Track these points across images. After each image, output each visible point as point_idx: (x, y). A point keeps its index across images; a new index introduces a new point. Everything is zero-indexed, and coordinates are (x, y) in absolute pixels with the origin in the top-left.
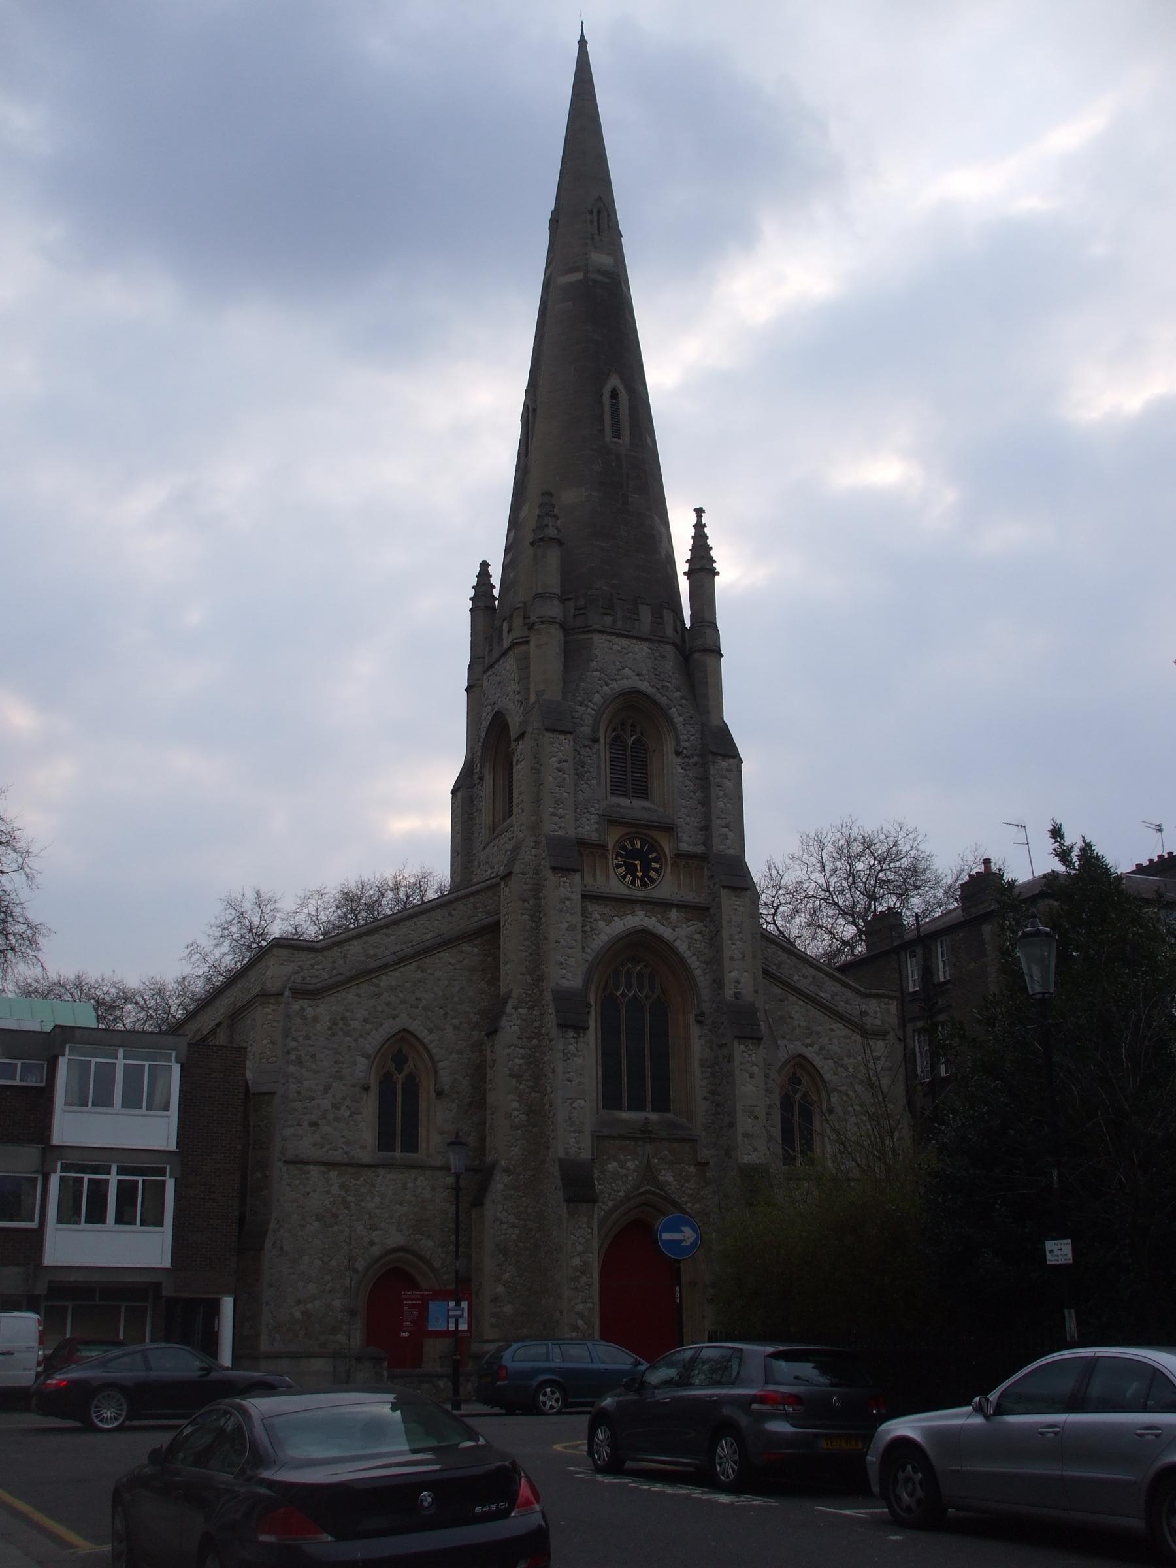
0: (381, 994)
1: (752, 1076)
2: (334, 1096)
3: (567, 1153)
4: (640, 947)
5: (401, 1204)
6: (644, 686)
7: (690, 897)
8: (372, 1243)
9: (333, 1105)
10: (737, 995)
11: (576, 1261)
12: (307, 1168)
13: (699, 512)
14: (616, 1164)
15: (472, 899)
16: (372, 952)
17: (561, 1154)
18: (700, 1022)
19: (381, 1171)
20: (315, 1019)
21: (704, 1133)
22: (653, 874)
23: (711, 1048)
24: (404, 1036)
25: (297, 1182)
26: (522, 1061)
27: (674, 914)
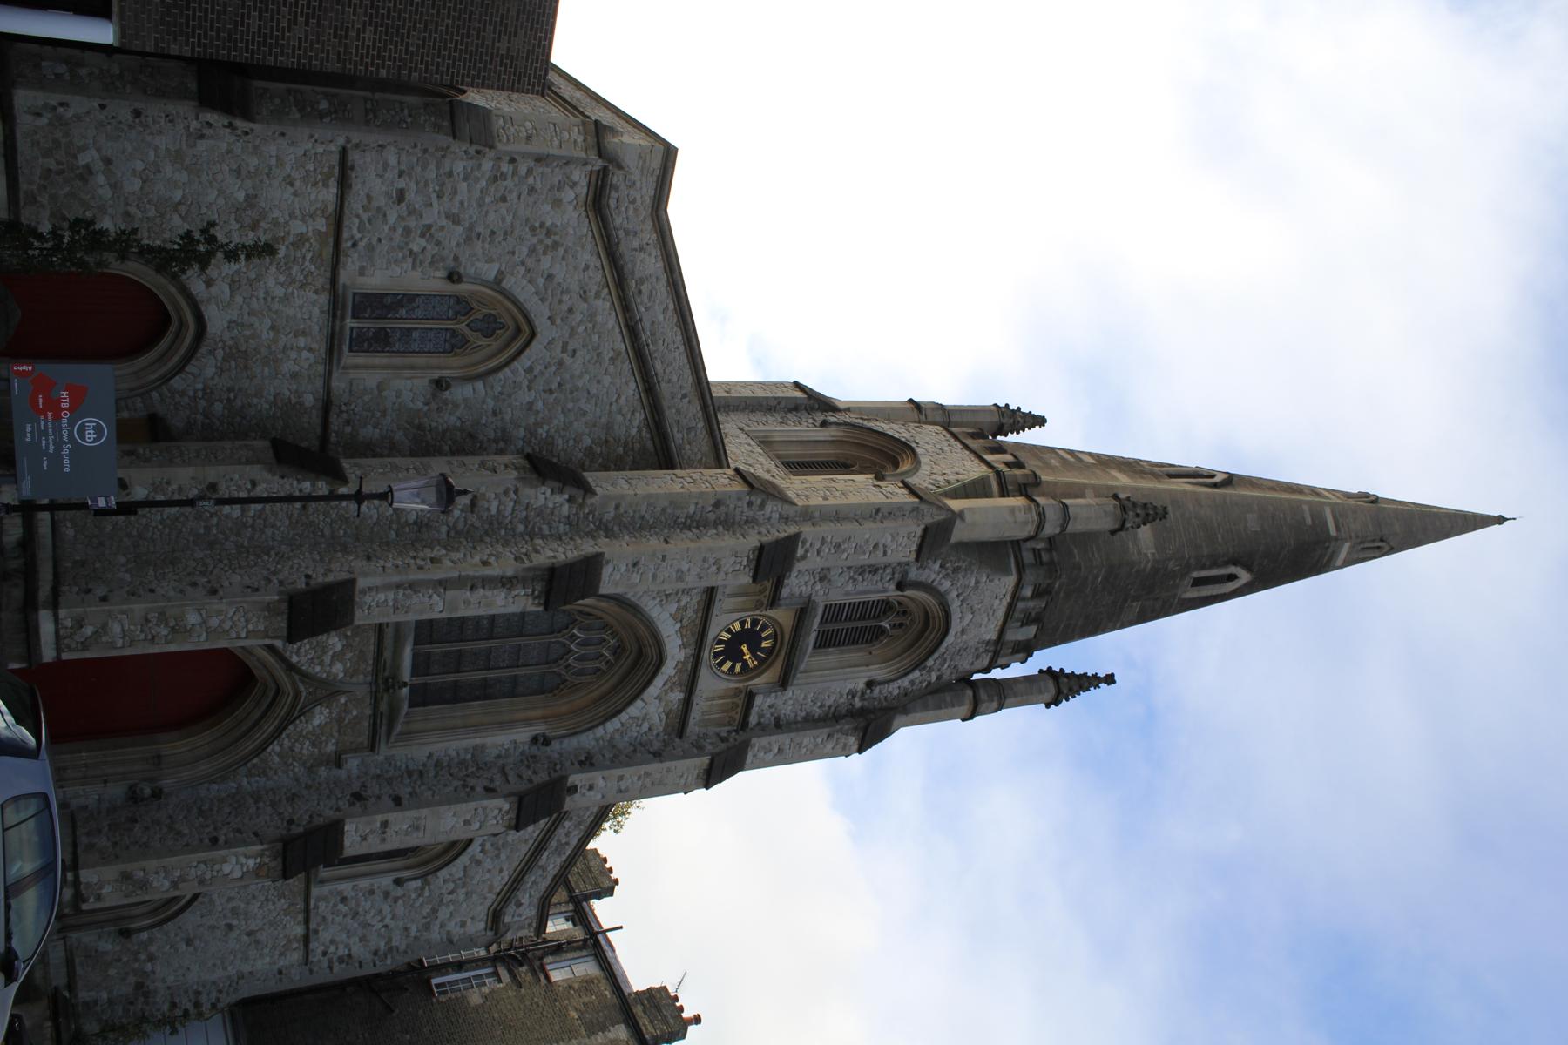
0: (585, 300)
1: (467, 823)
2: (442, 228)
3: (363, 592)
4: (641, 658)
5: (273, 328)
6: (950, 639)
7: (696, 714)
8: (209, 283)
9: (429, 227)
10: (573, 789)
11: (193, 618)
12: (333, 183)
13: (1110, 679)
14: (339, 647)
15: (701, 425)
16: (645, 288)
17: (362, 583)
18: (535, 740)
19: (324, 299)
20: (557, 203)
21: (381, 758)
22: (728, 664)
23: (499, 756)
24: (524, 333)
25: (310, 167)
26: (494, 511)
27: (677, 696)
